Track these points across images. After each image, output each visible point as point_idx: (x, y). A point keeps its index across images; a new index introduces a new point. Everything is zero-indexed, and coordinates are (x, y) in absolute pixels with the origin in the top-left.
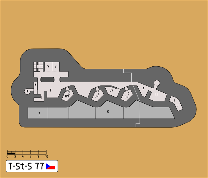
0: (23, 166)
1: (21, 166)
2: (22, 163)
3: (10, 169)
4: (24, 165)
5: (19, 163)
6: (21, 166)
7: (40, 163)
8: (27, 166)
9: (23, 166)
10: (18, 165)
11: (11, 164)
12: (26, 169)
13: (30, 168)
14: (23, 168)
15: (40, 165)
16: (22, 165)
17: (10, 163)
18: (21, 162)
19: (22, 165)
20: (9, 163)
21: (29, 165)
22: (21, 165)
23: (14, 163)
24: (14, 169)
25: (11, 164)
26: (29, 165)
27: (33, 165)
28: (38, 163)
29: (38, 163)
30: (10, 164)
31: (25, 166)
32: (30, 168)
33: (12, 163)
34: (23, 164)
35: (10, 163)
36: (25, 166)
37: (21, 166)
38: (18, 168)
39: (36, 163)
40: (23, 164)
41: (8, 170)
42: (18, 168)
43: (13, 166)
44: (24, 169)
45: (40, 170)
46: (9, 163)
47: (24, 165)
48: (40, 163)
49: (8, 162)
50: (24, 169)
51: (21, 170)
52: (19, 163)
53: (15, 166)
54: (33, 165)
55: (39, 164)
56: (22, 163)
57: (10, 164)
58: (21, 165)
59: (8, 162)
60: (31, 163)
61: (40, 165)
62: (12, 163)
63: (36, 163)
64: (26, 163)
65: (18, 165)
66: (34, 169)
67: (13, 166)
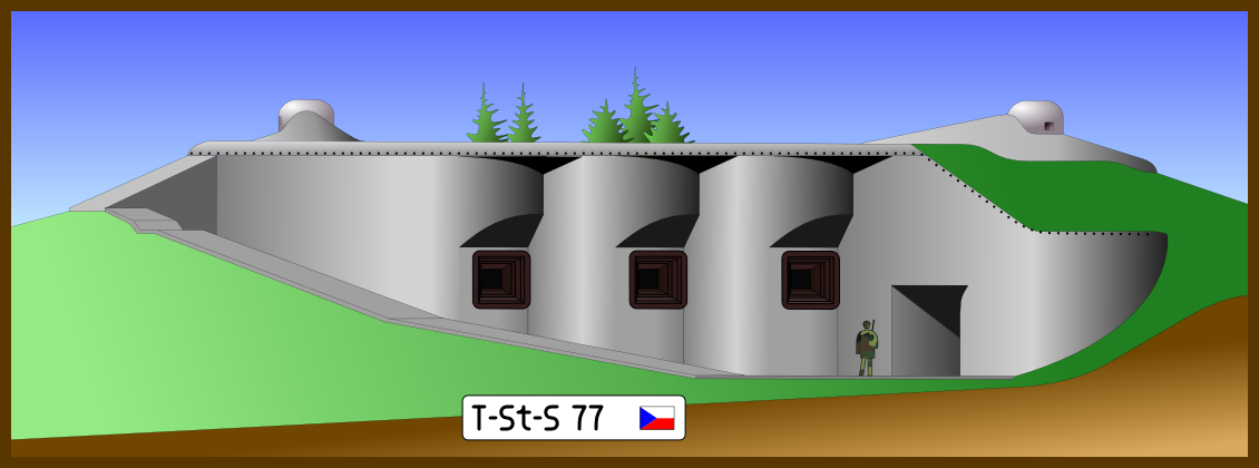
0: (527, 416)
1: (518, 419)
2: (524, 407)
3: (479, 429)
4: (529, 412)
5: (512, 407)
6: (520, 416)
7: (591, 407)
8: (540, 418)
9: (527, 416)
10: (506, 412)
11: (482, 410)
12: (538, 431)
13: (552, 424)
14: (527, 425)
15: (590, 414)
16: (523, 412)
17: (479, 408)
18: (518, 402)
19: (523, 412)
20: (474, 407)
21: (551, 412)
22: (518, 412)
23: (493, 405)
24: (492, 431)
25: (482, 410)
26: (551, 412)
27: (565, 409)
28: (584, 408)
29: (584, 408)
30: (476, 410)
31: (535, 418)
32: (552, 424)
33: (484, 407)
34: (527, 409)
35: (479, 408)
36: (535, 418)
37: (520, 416)
38: (508, 424)
39: (574, 407)
40: (527, 409)
41: (470, 432)
42: (508, 424)
43: (491, 418)
44: (529, 429)
45: (588, 433)
46: (474, 407)
47: (529, 412)
48: (591, 407)
49: (469, 402)
50: (529, 429)
51: (518, 433)
52: (512, 407)
53: (496, 418)
54: (565, 409)
55: (588, 408)
56: (524, 407)
57: (476, 410)
58: (518, 412)
59: (469, 402)
60: (557, 407)
61: (590, 414)
62: (484, 407)
63: (574, 407)
64: (536, 405)
65: (506, 412)
66: (567, 431)
67: (491, 418)
